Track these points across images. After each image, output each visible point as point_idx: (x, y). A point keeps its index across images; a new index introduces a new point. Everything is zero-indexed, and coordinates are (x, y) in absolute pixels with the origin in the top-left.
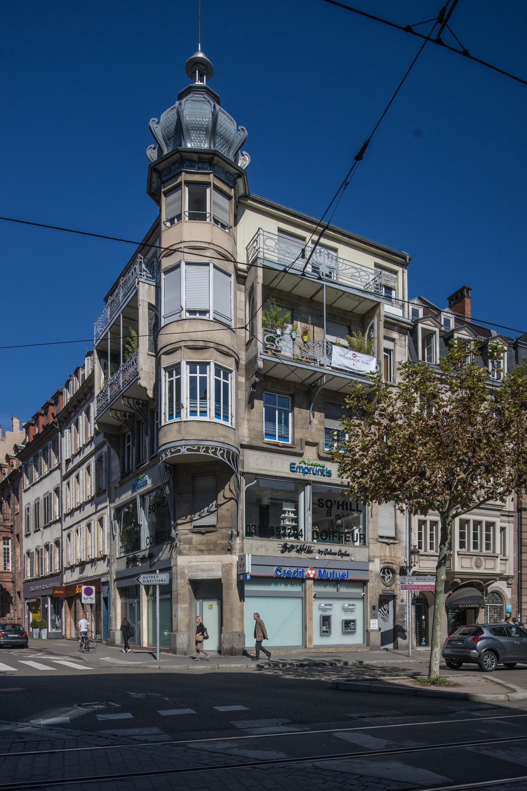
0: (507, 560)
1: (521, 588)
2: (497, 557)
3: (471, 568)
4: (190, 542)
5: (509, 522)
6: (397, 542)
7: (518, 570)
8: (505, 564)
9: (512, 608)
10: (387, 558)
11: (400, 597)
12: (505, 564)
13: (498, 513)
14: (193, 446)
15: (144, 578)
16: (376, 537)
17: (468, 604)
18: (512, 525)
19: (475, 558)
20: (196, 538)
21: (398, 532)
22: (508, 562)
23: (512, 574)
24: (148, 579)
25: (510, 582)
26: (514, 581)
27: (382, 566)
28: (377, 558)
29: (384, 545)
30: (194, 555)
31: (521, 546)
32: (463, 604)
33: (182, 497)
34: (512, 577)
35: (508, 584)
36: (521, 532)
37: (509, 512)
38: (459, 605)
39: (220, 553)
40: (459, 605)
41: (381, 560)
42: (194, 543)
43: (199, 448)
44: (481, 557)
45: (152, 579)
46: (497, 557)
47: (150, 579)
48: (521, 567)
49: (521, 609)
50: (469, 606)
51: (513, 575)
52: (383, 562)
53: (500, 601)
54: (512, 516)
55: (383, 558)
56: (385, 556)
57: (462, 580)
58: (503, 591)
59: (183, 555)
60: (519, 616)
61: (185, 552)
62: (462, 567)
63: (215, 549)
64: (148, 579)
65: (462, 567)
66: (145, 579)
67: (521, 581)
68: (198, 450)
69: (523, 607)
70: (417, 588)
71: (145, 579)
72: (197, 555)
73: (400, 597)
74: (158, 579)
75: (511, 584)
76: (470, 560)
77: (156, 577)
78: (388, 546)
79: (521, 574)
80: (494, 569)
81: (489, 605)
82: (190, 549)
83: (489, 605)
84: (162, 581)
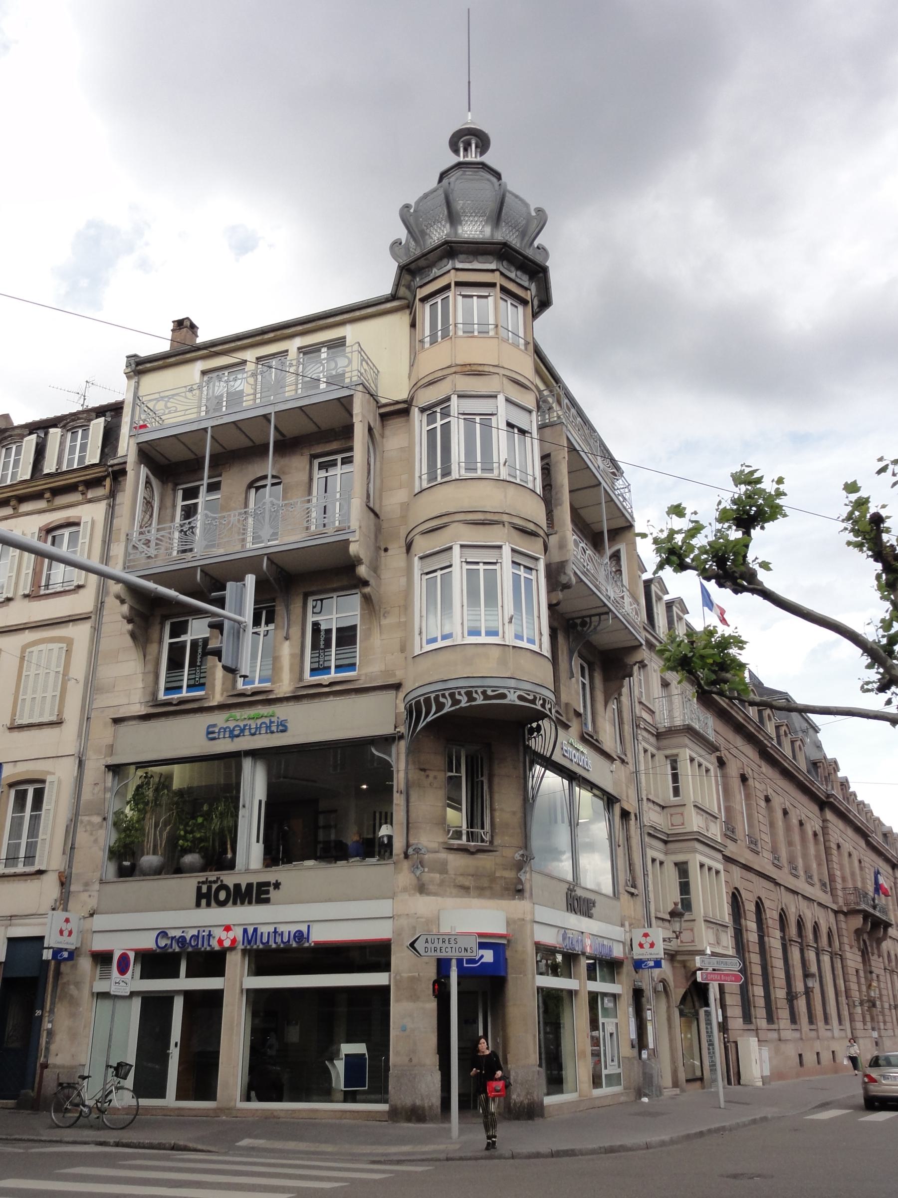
4: (443, 868)
14: (528, 692)
15: (427, 942)
20: (456, 862)
24: (436, 945)
30: (451, 896)
33: (428, 776)
39: (501, 896)
42: (451, 872)
43: (535, 698)
45: (444, 946)
47: (441, 944)
59: (429, 894)
61: (432, 888)
63: (491, 888)
64: (436, 945)
66: (429, 945)
68: (533, 701)
71: (429, 945)
72: (455, 897)
74: (457, 946)
77: (452, 941)
82: (442, 883)
84: (466, 950)
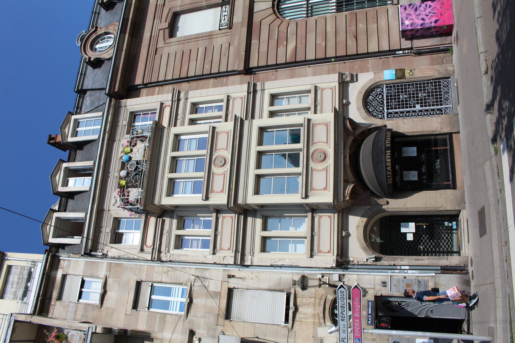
0: (316, 87)
1: (357, 55)
2: (309, 120)
3: (326, 169)
5: (263, 90)
6: (292, 291)
7: (331, 62)
8: (323, 90)
9: (389, 68)
10: (317, 312)
11: (377, 288)
12: (323, 90)
13: (246, 123)
16: (285, 331)
17: (387, 167)
18: (268, 84)
19: (312, 164)
21: (278, 288)
22: (319, 85)
23: (335, 77)
25: (348, 79)
26: (346, 67)
27: (329, 323)
28: (315, 331)
29: (298, 315)
31: (296, 62)
32: (387, 178)
34: (341, 75)
35: (352, 81)
36: (277, 65)
37: (249, 93)
38: (388, 185)
40: (388, 185)
41: (320, 325)
44: (311, 151)
46: (309, 120)
48: (326, 58)
49: (390, 51)
50: (389, 168)
51: (337, 75)
52: (322, 321)
53: (379, 90)
54: (255, 85)
55: (317, 321)
56: (314, 315)
57: (346, 182)
58: (363, 87)
60: (401, 52)
62: (325, 189)
65: (325, 189)
67: (347, 56)
69: (387, 49)
70: (358, 321)
73: (377, 288)
75: (352, 76)
76: (314, 172)
78: (300, 309)
79: (336, 57)
80: (327, 125)
81: (386, 110)
83: (386, 110)
